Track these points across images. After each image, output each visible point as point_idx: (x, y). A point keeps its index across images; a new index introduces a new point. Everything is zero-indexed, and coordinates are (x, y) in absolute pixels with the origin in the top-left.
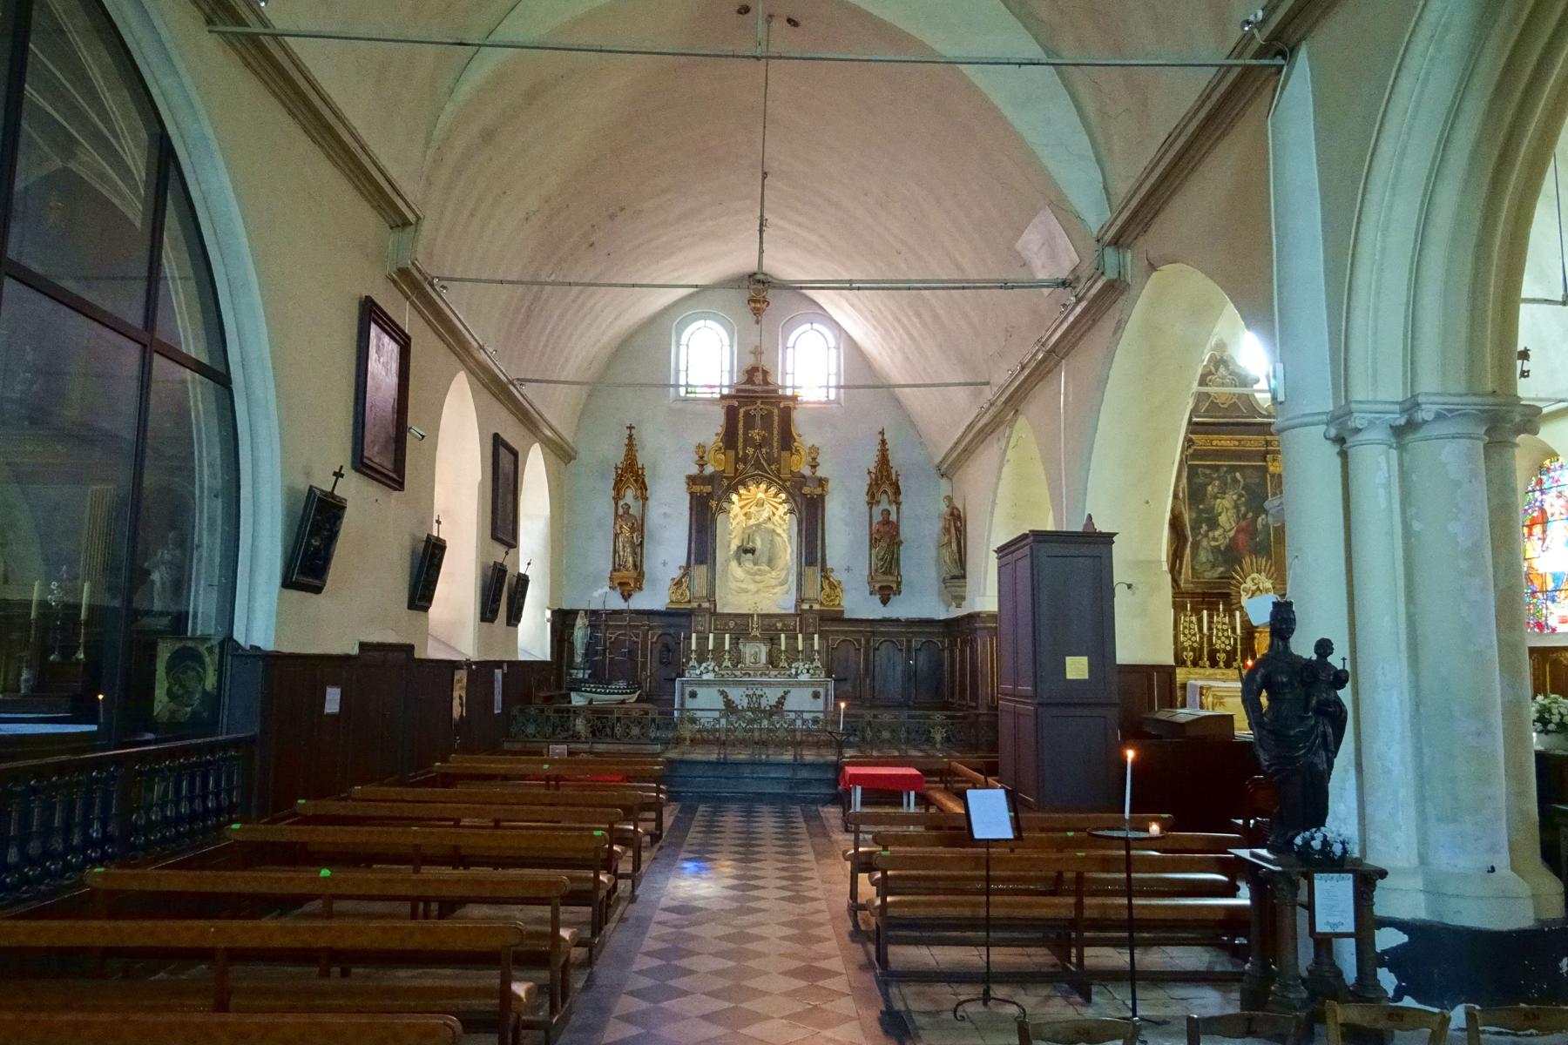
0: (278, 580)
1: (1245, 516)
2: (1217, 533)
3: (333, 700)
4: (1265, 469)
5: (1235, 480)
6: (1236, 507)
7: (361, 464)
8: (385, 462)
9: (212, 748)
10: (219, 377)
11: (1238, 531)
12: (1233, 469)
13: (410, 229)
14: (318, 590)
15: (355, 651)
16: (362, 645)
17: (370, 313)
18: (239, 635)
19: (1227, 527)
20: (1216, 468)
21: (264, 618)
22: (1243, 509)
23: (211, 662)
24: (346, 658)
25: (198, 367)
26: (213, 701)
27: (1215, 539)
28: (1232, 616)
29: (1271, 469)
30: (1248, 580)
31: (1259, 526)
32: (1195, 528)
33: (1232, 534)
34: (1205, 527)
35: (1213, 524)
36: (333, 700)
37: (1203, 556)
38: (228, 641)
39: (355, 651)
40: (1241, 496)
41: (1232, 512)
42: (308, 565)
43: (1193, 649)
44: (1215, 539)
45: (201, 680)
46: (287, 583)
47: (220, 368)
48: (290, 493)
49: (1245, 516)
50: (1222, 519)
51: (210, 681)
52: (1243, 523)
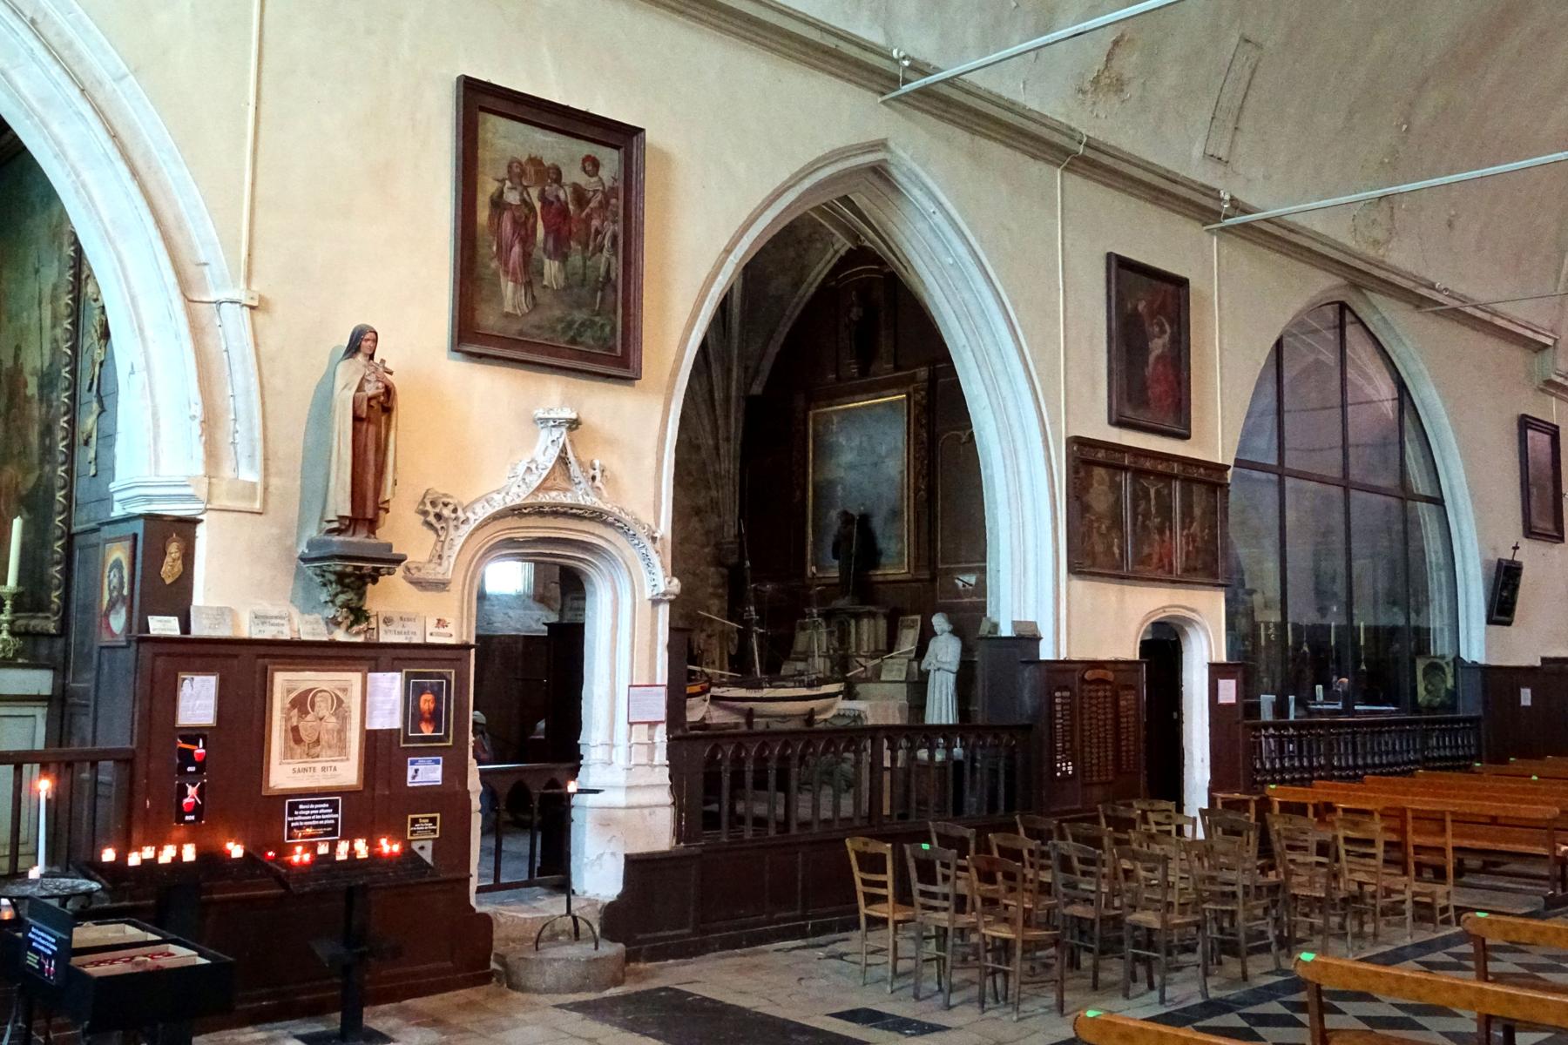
0: (1484, 620)
3: (1526, 697)
7: (1530, 532)
8: (1549, 526)
9: (1453, 721)
10: (1438, 501)
13: (1548, 353)
14: (1509, 624)
15: (1539, 664)
16: (1544, 660)
17: (1525, 423)
18: (1463, 655)
21: (1477, 643)
23: (1449, 671)
24: (1531, 669)
25: (1428, 500)
26: (1453, 694)
36: (1526, 697)
38: (1457, 659)
39: (1539, 664)
42: (1501, 609)
45: (1444, 682)
46: (1490, 621)
47: (1436, 495)
48: (1486, 564)
51: (1450, 683)
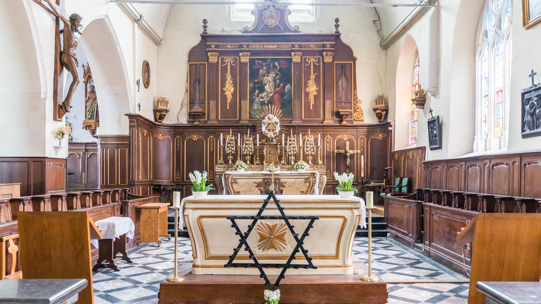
1: (279, 86)
2: (263, 95)
4: (291, 59)
5: (275, 67)
6: (275, 80)
11: (274, 93)
12: (274, 60)
19: (269, 91)
20: (265, 60)
22: (278, 81)
27: (262, 98)
28: (255, 139)
29: (294, 60)
30: (266, 117)
31: (286, 91)
32: (252, 92)
33: (271, 95)
34: (257, 92)
35: (262, 90)
37: (255, 107)
40: (277, 75)
41: (272, 83)
43: (232, 155)
44: (262, 98)
49: (279, 86)
50: (267, 87)
52: (278, 89)
